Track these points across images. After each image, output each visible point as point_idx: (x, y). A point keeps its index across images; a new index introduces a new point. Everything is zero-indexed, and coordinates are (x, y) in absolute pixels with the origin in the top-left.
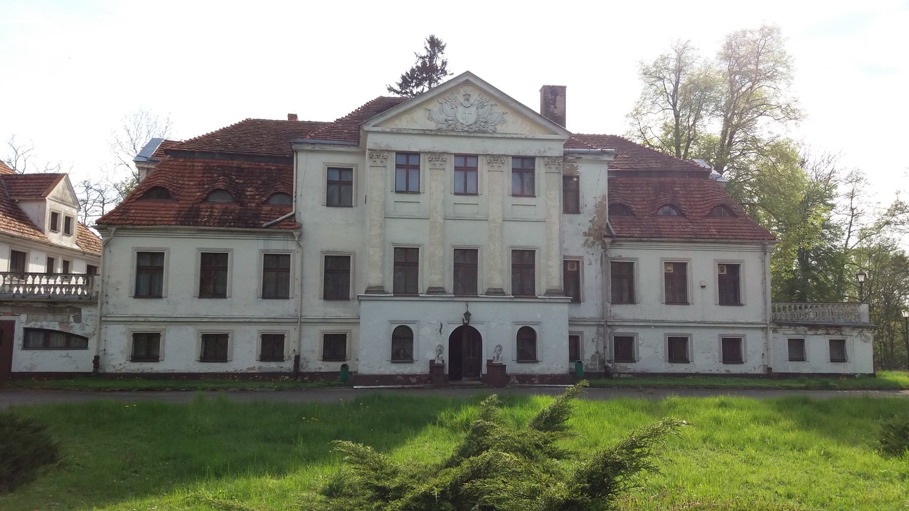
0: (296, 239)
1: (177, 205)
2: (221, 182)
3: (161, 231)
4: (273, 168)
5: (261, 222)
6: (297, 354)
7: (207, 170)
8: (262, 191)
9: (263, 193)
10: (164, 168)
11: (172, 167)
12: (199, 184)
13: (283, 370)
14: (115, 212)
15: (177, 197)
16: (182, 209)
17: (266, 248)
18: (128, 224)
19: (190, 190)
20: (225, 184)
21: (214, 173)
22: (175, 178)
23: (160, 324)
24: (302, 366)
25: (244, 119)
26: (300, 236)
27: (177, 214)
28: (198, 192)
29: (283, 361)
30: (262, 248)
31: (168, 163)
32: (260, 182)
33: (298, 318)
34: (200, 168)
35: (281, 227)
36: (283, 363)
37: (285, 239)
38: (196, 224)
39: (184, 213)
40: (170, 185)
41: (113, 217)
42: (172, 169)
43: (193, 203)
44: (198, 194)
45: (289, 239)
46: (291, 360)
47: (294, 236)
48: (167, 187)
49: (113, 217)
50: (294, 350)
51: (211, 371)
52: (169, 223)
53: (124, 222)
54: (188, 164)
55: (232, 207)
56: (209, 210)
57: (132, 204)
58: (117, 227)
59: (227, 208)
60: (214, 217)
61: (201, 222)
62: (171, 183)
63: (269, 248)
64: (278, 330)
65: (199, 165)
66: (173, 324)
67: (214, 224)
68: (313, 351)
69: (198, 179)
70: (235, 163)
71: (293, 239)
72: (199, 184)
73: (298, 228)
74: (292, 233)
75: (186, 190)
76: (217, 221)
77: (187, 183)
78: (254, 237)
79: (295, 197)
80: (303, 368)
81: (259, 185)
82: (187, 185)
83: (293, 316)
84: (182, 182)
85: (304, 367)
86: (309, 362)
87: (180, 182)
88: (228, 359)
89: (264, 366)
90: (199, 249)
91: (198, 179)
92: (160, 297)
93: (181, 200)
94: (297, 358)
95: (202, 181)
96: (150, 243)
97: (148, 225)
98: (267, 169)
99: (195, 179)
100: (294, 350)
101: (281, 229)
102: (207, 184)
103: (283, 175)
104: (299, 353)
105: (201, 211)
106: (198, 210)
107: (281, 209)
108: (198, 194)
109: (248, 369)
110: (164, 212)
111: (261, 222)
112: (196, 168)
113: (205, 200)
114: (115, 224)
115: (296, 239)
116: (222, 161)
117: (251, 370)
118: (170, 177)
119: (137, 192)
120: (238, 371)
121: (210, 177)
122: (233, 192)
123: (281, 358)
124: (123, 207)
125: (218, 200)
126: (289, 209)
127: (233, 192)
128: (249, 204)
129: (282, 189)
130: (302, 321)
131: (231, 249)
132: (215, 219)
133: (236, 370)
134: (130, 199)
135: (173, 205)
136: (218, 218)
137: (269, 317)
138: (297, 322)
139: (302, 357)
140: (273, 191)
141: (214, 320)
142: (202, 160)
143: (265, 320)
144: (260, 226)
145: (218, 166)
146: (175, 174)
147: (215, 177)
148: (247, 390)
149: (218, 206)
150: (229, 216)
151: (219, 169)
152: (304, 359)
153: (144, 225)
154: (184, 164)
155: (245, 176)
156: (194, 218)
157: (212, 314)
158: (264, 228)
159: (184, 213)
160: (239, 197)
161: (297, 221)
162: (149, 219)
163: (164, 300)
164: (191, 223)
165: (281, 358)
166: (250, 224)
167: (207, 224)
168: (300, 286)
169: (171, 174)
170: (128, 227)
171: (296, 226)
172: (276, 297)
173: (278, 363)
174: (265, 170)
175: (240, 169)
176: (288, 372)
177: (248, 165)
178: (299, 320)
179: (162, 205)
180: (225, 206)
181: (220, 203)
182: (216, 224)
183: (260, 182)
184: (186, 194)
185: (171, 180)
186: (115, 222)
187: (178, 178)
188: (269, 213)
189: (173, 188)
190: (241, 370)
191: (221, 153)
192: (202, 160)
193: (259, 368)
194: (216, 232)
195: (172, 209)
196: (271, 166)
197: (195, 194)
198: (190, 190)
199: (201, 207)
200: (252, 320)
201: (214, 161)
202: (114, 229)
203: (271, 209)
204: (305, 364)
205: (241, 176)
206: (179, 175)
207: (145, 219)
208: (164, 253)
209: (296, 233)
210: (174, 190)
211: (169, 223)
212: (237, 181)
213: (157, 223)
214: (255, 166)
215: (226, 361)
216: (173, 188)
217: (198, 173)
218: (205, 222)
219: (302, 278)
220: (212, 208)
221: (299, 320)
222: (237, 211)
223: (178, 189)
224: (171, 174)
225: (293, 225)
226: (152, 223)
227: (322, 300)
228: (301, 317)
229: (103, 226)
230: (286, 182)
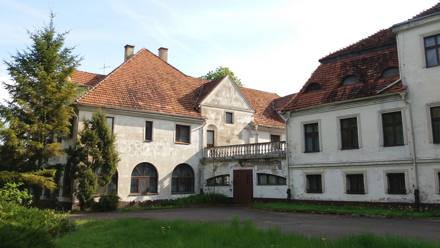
0: (403, 98)
1: (325, 92)
2: (351, 71)
3: (314, 110)
4: (387, 52)
5: (376, 91)
6: (416, 189)
7: (344, 66)
8: (379, 70)
9: (379, 71)
10: (318, 71)
11: (323, 70)
12: (338, 76)
13: (407, 201)
14: (291, 103)
15: (324, 87)
16: (327, 94)
17: (382, 109)
18: (296, 109)
19: (332, 81)
20: (353, 71)
21: (348, 67)
22: (325, 76)
23: (320, 168)
24: (422, 199)
25: (379, 31)
26: (406, 95)
27: (323, 97)
28: (337, 81)
29: (406, 194)
30: (379, 110)
31: (321, 68)
32: (377, 64)
33: (413, 160)
34: (339, 66)
35: (391, 91)
36: (406, 195)
37: (395, 100)
38: (334, 101)
39: (327, 96)
40: (321, 80)
41: (289, 106)
42: (323, 71)
43: (334, 88)
44: (337, 82)
45: (398, 99)
46: (412, 193)
47: (401, 96)
48: (318, 82)
49: (289, 106)
50: (414, 185)
51: (355, 200)
52: (318, 103)
53: (294, 108)
54: (332, 65)
55: (358, 85)
56: (343, 91)
57: (300, 97)
58: (291, 111)
59: (354, 87)
60: (345, 94)
61: (337, 99)
62: (321, 79)
63: (384, 109)
64: (399, 170)
65: (339, 64)
66: (327, 168)
67: (345, 98)
68: (430, 186)
69: (338, 73)
70: (361, 56)
71: (401, 99)
72: (338, 76)
73: (403, 90)
74: (399, 95)
75: (330, 82)
76: (347, 96)
77: (331, 77)
78: (372, 102)
79: (400, 67)
80: (423, 200)
81: (377, 66)
82: (331, 78)
83: (409, 158)
84: (328, 77)
85: (423, 199)
86: (428, 195)
87: (327, 77)
88: (365, 192)
89: (391, 198)
90: (337, 117)
91: (338, 73)
92: (319, 151)
93: (327, 88)
94: (417, 192)
95: (340, 73)
96: (309, 118)
97: (307, 107)
98: (383, 54)
99: (336, 73)
100: (414, 185)
101: (390, 93)
102: (342, 75)
103: (394, 55)
104: (418, 188)
105: (338, 92)
106: (337, 92)
107: (392, 79)
108: (337, 82)
109: (380, 199)
110: (316, 98)
111: (376, 91)
112: (337, 66)
113: (341, 85)
114: (290, 110)
115: (403, 98)
116: (353, 58)
117: (382, 200)
118: (321, 76)
119: (303, 89)
120: (373, 201)
121: (345, 70)
122: (358, 75)
123: (403, 192)
124: (296, 99)
125: (349, 83)
126: (399, 77)
127: (358, 75)
128: (369, 81)
129: (391, 64)
130: (417, 162)
131: (358, 114)
132: (346, 95)
133: (372, 200)
134: (299, 94)
135: (322, 92)
136: (348, 94)
137: (390, 160)
138: (413, 163)
139: (421, 190)
140: (385, 68)
141: (352, 164)
142: (341, 61)
143: (388, 163)
144: (374, 94)
145: (350, 62)
146: (324, 74)
147: (348, 69)
148: (365, 216)
149: (349, 87)
150: (356, 91)
151: (351, 63)
152: (423, 192)
153: (304, 107)
154: (330, 66)
155: (368, 63)
156: (332, 98)
157: (351, 161)
158: (378, 94)
159: (327, 96)
160: (363, 77)
161: (403, 85)
162: (307, 103)
163: (321, 153)
164: (331, 101)
165: (403, 192)
166: (368, 94)
167: (340, 99)
168: (412, 135)
169: (322, 74)
170: (297, 110)
171: (402, 89)
172: (395, 144)
173: (403, 195)
174: (381, 56)
175: (364, 60)
176: (411, 202)
177: (369, 55)
178: (414, 161)
179: (316, 93)
180: (353, 86)
181: (350, 84)
182: (346, 99)
183: (377, 64)
184: (330, 84)
185: (321, 78)
186: (290, 109)
187: (326, 76)
188: (383, 84)
189: (322, 82)
190: (375, 200)
191: (352, 53)
192: (341, 61)
193: (388, 199)
194: (347, 104)
195: (322, 95)
196: (386, 51)
197: (335, 83)
198: (332, 81)
199: (338, 90)
200: (378, 163)
201: (348, 59)
202: (289, 113)
203: (385, 80)
204: (424, 197)
205: (365, 64)
206: (327, 73)
207: (305, 104)
208: (318, 123)
209: (402, 94)
210: (323, 83)
211: (318, 103)
212: (362, 68)
213: (312, 105)
214: (375, 55)
215: (364, 194)
216: (322, 82)
217: (338, 70)
218: (340, 98)
219: (412, 128)
220: (345, 89)
221: (414, 161)
222: (361, 87)
223: (325, 82)
224: (322, 74)
225: (400, 88)
226: (309, 105)
227: (432, 144)
228: (415, 159)
229: (283, 112)
230: (395, 59)
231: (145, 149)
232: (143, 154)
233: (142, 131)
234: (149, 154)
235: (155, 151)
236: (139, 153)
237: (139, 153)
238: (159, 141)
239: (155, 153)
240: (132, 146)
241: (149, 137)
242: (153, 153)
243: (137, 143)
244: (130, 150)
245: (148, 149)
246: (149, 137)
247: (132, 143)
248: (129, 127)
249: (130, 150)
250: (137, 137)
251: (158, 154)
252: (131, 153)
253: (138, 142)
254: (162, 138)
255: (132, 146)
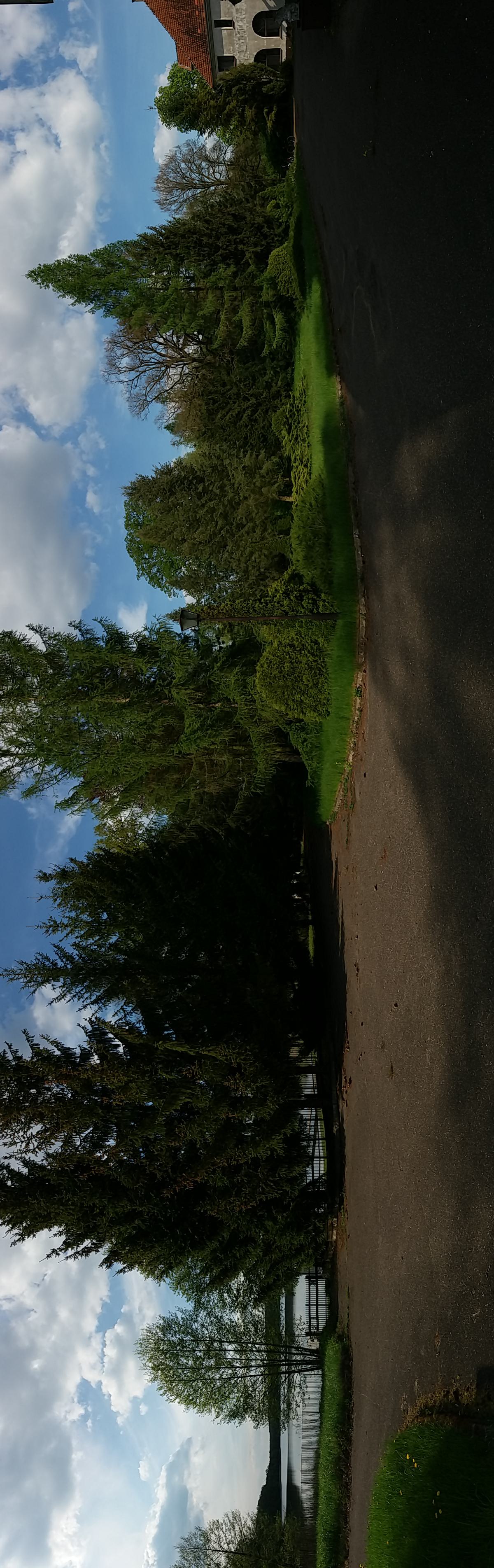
231: (240, 26)
232: (245, 28)
233: (225, 30)
234: (245, 22)
235: (241, 17)
236: (244, 32)
237: (244, 32)
238: (232, 13)
239: (243, 16)
240: (239, 40)
241: (230, 23)
242: (244, 18)
243: (236, 34)
244: (243, 41)
245: (241, 23)
246: (230, 23)
247: (237, 39)
248: (224, 43)
249: (243, 41)
250: (230, 35)
251: (244, 13)
252: (245, 39)
253: (235, 34)
254: (229, 9)
255: (239, 40)
